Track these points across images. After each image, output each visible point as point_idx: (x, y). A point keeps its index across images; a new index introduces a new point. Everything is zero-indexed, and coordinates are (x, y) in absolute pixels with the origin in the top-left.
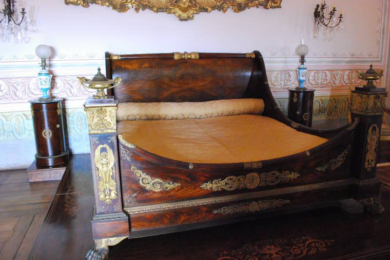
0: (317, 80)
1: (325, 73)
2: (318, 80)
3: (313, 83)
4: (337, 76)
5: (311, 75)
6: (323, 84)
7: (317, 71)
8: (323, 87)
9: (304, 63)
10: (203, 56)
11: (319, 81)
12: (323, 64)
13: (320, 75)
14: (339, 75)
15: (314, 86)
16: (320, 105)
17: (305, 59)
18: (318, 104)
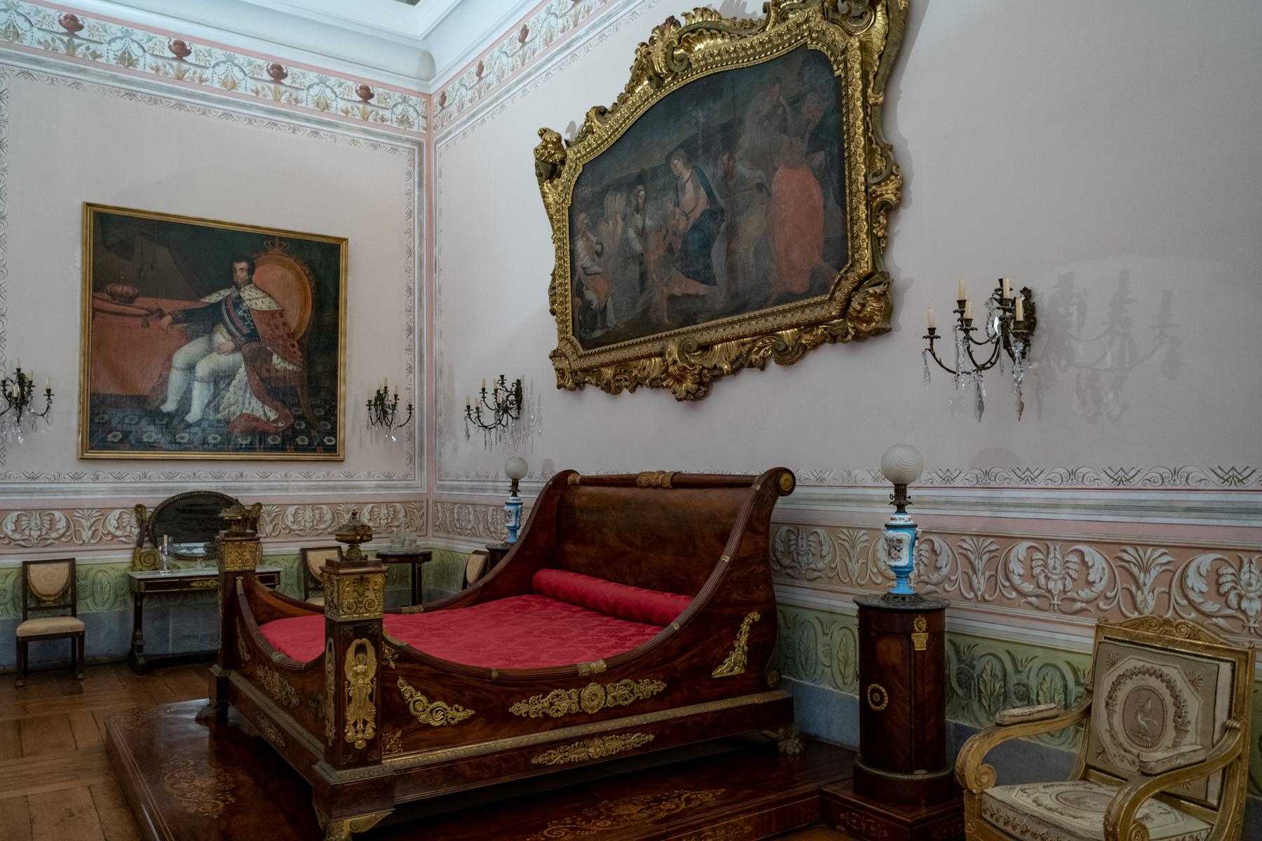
0: (1042, 580)
1: (1082, 554)
2: (1047, 578)
3: (1028, 587)
4: (1146, 570)
5: (1013, 554)
6: (1074, 600)
7: (1042, 544)
8: (1076, 613)
9: (907, 509)
10: (680, 482)
11: (1051, 585)
12: (1066, 515)
13: (1055, 559)
14: (1154, 573)
15: (1033, 600)
16: (1066, 687)
17: (909, 492)
18: (1059, 684)
